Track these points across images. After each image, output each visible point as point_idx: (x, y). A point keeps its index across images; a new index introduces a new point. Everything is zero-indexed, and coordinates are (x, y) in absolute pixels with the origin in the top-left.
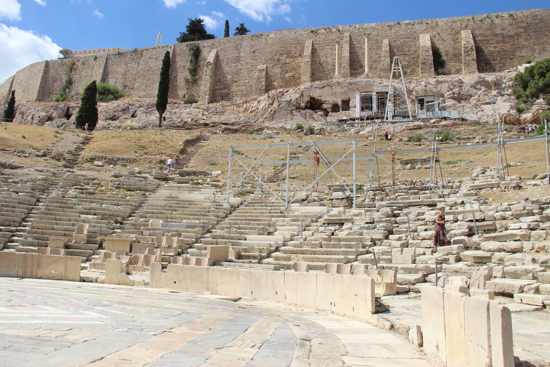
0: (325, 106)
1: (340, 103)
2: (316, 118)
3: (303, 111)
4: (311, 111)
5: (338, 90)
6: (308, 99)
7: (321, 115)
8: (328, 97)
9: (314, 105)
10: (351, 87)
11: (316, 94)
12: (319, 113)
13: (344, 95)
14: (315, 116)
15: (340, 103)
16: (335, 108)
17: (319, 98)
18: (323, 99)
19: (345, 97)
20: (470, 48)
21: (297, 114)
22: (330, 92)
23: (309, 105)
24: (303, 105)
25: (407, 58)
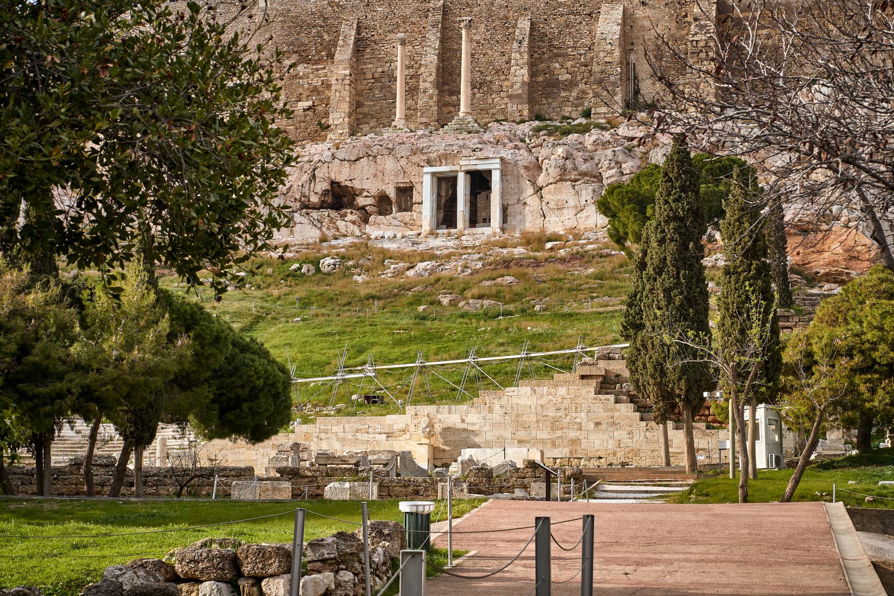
0: (361, 201)
1: (392, 194)
2: (343, 230)
3: (315, 214)
4: (333, 214)
5: (389, 164)
6: (325, 186)
7: (354, 223)
8: (369, 181)
9: (339, 198)
10: (415, 159)
11: (342, 174)
12: (350, 217)
13: (402, 176)
14: (341, 224)
15: (392, 194)
16: (383, 204)
17: (349, 184)
18: (357, 185)
19: (402, 180)
20: (702, 44)
21: (305, 220)
22: (372, 170)
23: (329, 199)
24: (314, 199)
25: (569, 64)
